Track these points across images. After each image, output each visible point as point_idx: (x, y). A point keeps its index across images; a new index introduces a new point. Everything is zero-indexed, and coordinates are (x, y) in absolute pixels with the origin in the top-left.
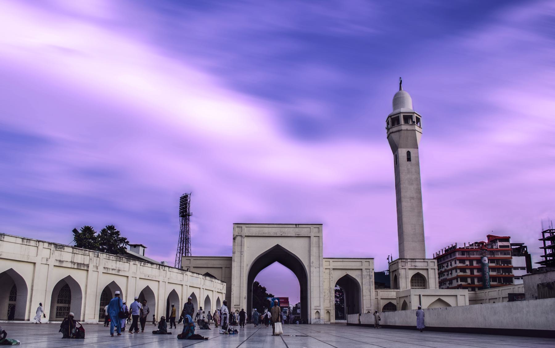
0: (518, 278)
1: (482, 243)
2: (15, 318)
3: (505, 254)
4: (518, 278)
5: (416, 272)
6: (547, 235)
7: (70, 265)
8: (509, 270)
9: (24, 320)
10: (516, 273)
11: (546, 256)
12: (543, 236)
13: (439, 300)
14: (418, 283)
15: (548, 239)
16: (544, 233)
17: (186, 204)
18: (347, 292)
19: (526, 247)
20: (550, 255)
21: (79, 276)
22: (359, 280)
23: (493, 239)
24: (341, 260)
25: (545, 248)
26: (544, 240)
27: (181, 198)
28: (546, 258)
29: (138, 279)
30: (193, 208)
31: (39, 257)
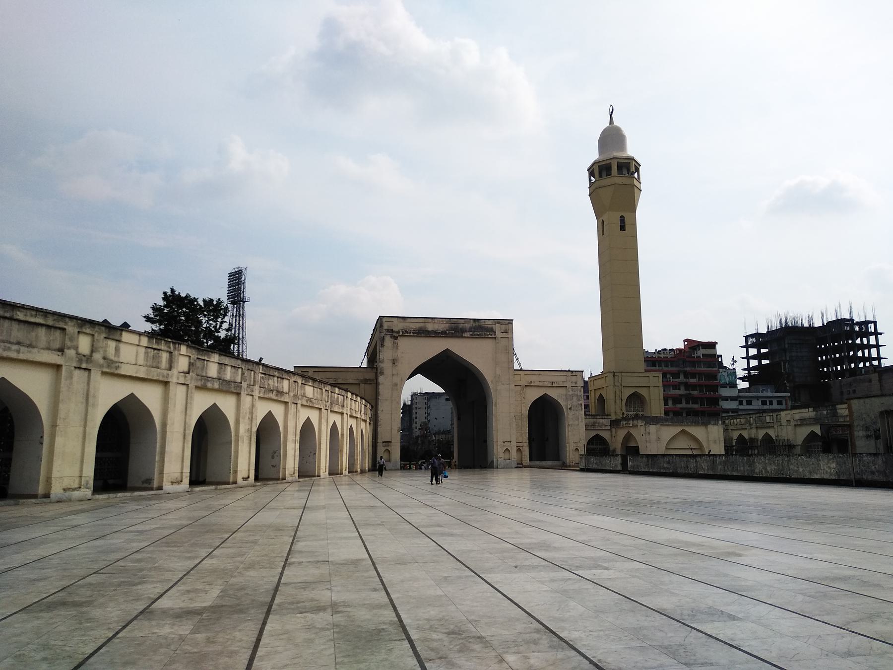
0: (726, 399)
1: (680, 350)
2: (129, 485)
3: (710, 366)
4: (726, 399)
5: (632, 391)
6: (750, 341)
7: (216, 386)
8: (715, 388)
9: (151, 489)
10: (725, 392)
11: (749, 369)
12: (746, 342)
13: (683, 432)
14: (634, 406)
15: (752, 346)
16: (747, 337)
17: (238, 284)
18: (544, 419)
19: (721, 356)
20: (754, 368)
21: (227, 405)
22: (562, 403)
23: (693, 346)
25: (748, 358)
26: (747, 347)
27: (231, 275)
28: (749, 373)
29: (299, 406)
30: (250, 290)
31: (175, 372)
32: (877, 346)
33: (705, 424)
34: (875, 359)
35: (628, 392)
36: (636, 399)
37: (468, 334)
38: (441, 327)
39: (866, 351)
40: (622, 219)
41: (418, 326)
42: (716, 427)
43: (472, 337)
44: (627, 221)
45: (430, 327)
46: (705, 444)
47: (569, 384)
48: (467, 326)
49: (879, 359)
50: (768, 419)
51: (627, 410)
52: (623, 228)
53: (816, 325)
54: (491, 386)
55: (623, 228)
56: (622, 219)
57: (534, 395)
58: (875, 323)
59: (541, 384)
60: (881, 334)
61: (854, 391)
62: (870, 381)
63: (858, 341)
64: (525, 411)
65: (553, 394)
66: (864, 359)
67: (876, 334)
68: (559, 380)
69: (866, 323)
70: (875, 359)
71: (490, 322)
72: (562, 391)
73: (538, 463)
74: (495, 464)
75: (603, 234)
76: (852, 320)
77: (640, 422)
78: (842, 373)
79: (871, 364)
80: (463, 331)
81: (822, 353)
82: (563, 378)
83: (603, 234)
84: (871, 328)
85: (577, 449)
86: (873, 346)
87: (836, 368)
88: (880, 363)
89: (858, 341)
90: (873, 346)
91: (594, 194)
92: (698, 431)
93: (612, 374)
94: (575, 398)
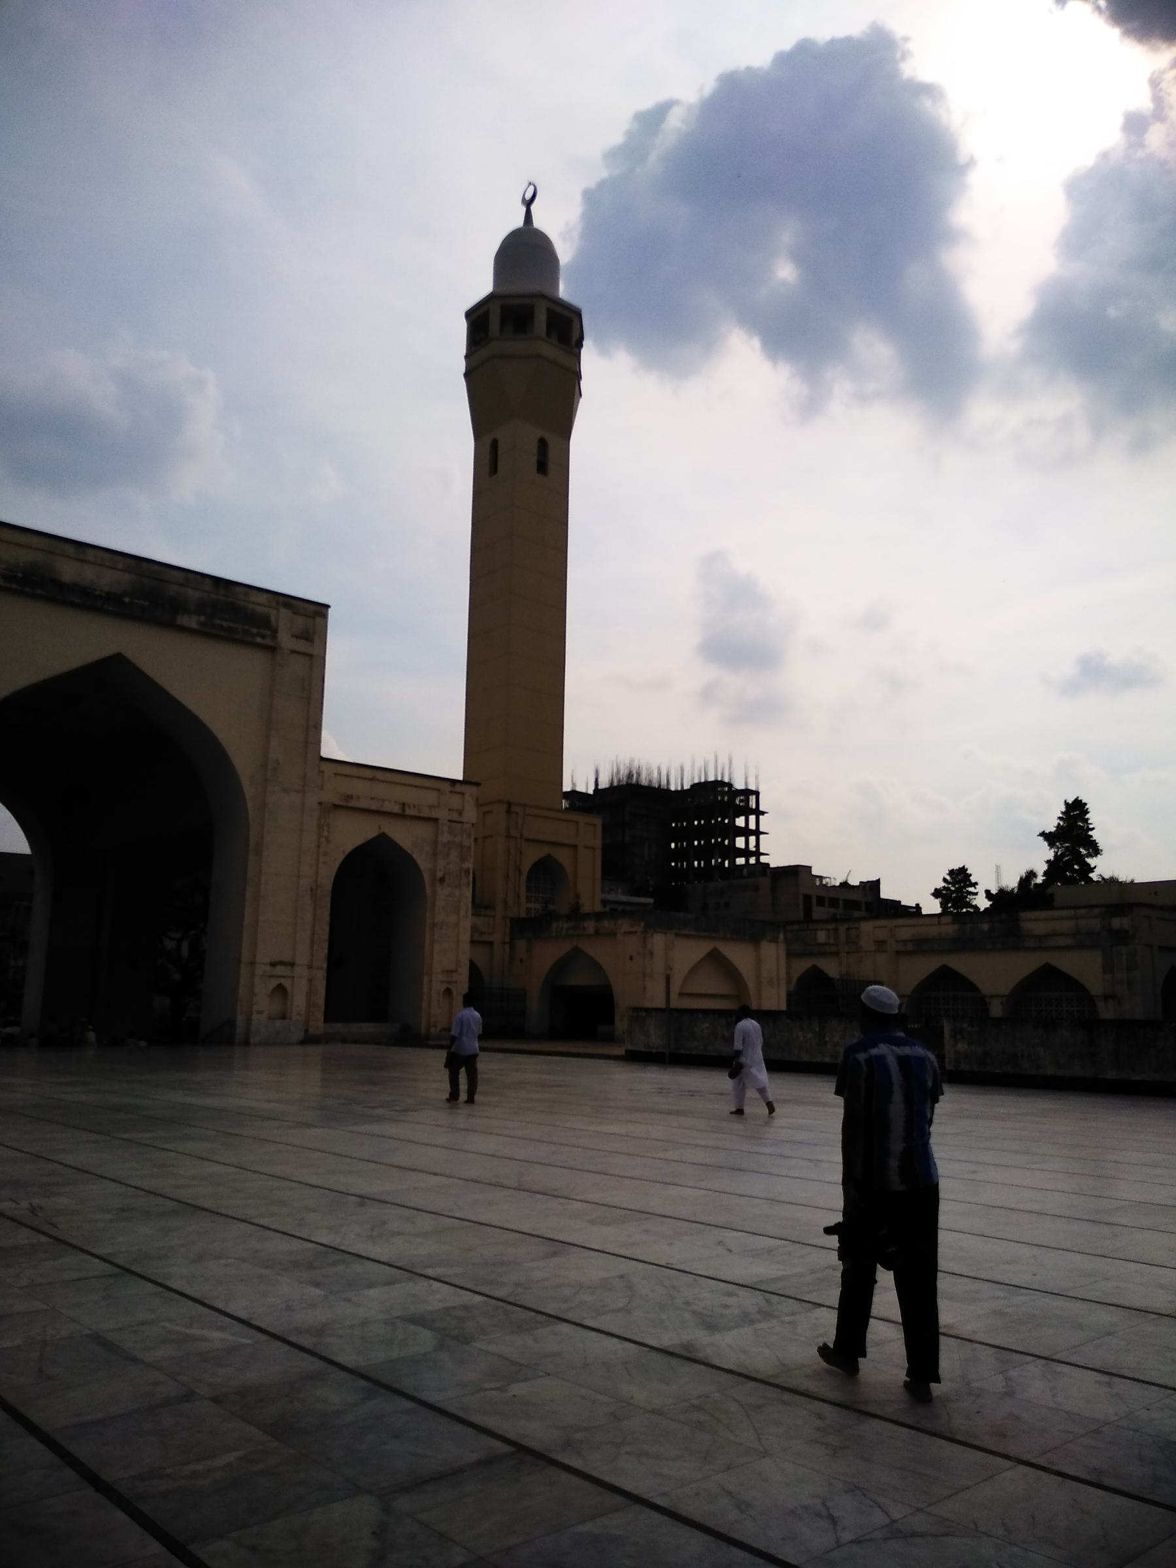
22: (423, 863)
24: (369, 774)
32: (757, 833)
33: (755, 940)
34: (752, 854)
35: (531, 856)
36: (546, 873)
37: (192, 621)
38: (107, 580)
39: (752, 839)
40: (543, 443)
41: (25, 557)
42: (773, 946)
43: (202, 633)
44: (552, 455)
45: (68, 571)
46: (751, 985)
47: (442, 814)
48: (193, 595)
49: (758, 854)
50: (821, 936)
51: (529, 900)
52: (542, 467)
53: (673, 788)
54: (249, 790)
55: (542, 467)
56: (543, 443)
57: (352, 833)
58: (757, 793)
59: (374, 806)
60: (763, 813)
61: (727, 905)
62: (757, 889)
63: (740, 822)
64: (328, 875)
65: (404, 836)
66: (746, 853)
67: (758, 813)
68: (422, 800)
69: (747, 792)
70: (752, 854)
71: (262, 599)
72: (423, 831)
73: (339, 1027)
74: (240, 1030)
75: (494, 469)
76: (730, 785)
77: (625, 925)
78: (707, 874)
79: (732, 862)
80: (177, 606)
81: (677, 836)
82: (431, 797)
83: (494, 469)
84: (753, 799)
85: (448, 992)
86: (752, 833)
87: (699, 864)
88: (758, 860)
89: (740, 822)
90: (752, 833)
91: (477, 376)
92: (739, 955)
93: (504, 807)
94: (454, 854)
